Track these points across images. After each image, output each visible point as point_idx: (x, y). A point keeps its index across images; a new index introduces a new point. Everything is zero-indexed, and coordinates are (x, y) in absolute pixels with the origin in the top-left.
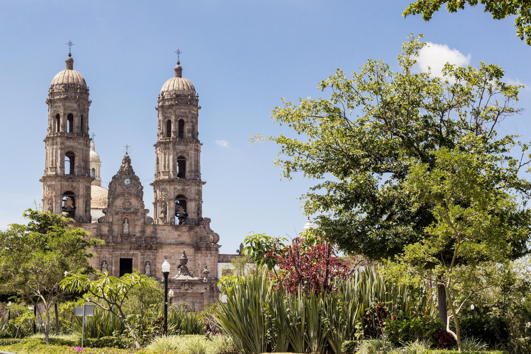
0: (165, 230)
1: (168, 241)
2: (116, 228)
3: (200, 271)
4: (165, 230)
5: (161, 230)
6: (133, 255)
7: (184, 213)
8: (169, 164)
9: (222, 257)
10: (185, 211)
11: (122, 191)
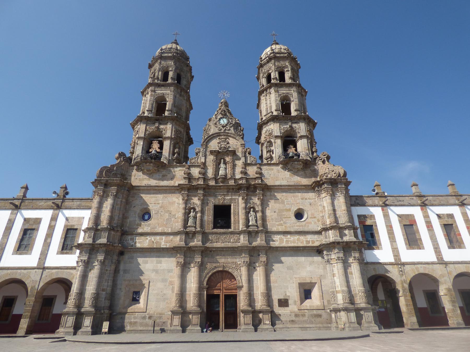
0: (273, 169)
1: (277, 183)
3: (327, 216)
6: (231, 199)
9: (354, 199)
10: (296, 150)
11: (217, 131)
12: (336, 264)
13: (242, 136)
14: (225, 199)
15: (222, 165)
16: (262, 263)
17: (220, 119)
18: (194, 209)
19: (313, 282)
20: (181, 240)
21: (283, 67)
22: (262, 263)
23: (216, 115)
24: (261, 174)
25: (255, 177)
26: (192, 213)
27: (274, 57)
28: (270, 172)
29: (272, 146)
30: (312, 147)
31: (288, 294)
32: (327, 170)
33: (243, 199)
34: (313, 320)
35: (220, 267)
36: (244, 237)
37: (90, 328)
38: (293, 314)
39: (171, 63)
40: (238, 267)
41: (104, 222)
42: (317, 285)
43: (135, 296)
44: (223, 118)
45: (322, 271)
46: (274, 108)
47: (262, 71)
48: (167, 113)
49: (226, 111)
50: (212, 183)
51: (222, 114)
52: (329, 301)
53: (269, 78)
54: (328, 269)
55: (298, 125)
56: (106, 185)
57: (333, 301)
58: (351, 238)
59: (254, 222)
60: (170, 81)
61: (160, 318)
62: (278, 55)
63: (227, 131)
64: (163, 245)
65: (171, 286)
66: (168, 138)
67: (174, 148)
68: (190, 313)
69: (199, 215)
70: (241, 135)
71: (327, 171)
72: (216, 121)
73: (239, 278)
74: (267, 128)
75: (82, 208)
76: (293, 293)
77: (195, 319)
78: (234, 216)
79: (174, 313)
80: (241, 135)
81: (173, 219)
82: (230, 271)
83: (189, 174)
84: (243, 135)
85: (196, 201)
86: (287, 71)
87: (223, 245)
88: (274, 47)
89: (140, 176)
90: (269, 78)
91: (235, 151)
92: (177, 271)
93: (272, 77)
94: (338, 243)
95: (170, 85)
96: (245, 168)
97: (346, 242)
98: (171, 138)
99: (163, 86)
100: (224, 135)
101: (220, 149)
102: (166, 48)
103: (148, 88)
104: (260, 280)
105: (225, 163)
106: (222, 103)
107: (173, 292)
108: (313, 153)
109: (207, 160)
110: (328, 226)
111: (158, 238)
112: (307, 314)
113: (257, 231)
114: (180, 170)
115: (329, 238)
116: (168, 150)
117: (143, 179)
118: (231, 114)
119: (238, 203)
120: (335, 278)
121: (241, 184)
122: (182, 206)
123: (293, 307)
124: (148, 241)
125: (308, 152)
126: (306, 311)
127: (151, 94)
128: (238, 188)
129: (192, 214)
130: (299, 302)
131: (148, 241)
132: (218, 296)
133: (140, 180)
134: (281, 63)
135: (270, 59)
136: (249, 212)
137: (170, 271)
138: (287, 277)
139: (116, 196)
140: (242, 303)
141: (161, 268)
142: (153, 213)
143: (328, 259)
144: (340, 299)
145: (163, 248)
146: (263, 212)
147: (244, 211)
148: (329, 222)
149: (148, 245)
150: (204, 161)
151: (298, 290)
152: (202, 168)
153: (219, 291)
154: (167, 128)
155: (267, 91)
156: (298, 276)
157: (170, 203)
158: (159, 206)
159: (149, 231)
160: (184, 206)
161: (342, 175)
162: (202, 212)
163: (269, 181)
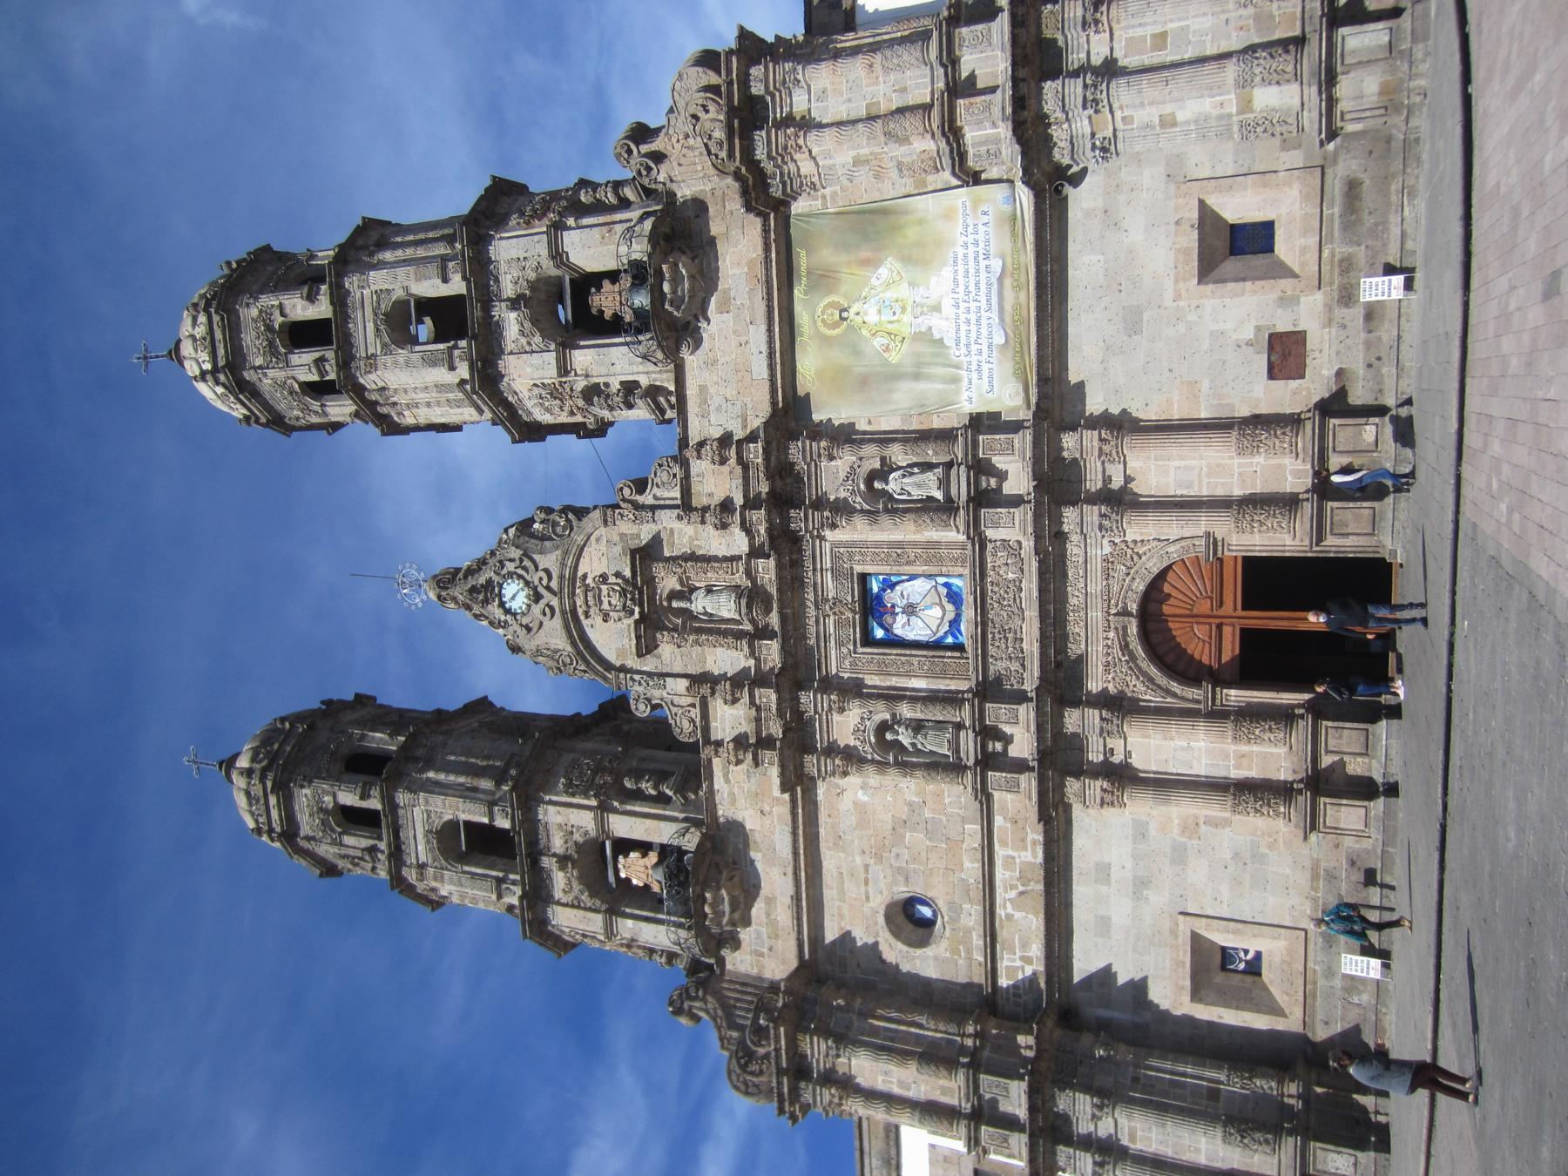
0: (703, 389)
1: (760, 369)
2: (727, 659)
3: (898, 151)
4: (703, 389)
5: (704, 415)
7: (626, 281)
8: (440, 387)
10: (613, 276)
11: (557, 622)
12: (1118, 114)
13: (570, 516)
14: (836, 600)
15: (700, 604)
16: (1106, 448)
17: (508, 611)
18: (883, 728)
19: (1194, 215)
20: (1013, 788)
21: (269, 328)
22: (1106, 448)
23: (491, 623)
24: (725, 440)
25: (739, 470)
26: (900, 738)
27: (232, 371)
28: (715, 402)
29: (607, 385)
30: (599, 208)
31: (1248, 333)
32: (691, 141)
33: (834, 526)
34: (1369, 221)
35: (1125, 628)
36: (996, 525)
37: (1360, 1154)
38: (1340, 313)
39: (304, 796)
40: (1127, 554)
41: (948, 1088)
42: (1212, 201)
43: (1242, 966)
44: (500, 595)
45: (1146, 173)
46: (441, 375)
47: (298, 419)
48: (503, 823)
49: (471, 582)
50: (772, 653)
51: (486, 602)
52: (1286, 145)
53: (320, 390)
54: (1137, 148)
55: (503, 267)
56: (799, 1070)
57: (1285, 128)
58: (995, 38)
59: (931, 478)
60: (374, 804)
61: (1331, 877)
62: (221, 351)
63: (554, 584)
64: (1033, 855)
65: (1203, 828)
66: (601, 824)
67: (638, 796)
68: (1315, 759)
69: (906, 711)
70: (568, 520)
71: (696, 142)
72: (517, 627)
73: (1171, 549)
74: (529, 404)
75: (893, 1152)
76: (1244, 309)
77: (1344, 744)
78: (908, 563)
79: (1313, 823)
80: (568, 520)
81: (928, 814)
82: (1140, 586)
83: (740, 742)
84: (565, 510)
85: (847, 725)
86: (283, 314)
87: (1032, 613)
88: (192, 369)
89: (758, 933)
90: (320, 390)
91: (633, 552)
92: (1139, 806)
93: (314, 377)
94: (1019, 102)
95: (392, 807)
96: (705, 509)
97: (1014, 64)
98: (604, 808)
99: (396, 830)
100: (574, 594)
101: (632, 613)
102: (252, 814)
103: (411, 887)
104: (1181, 458)
105: (687, 593)
106: (439, 597)
107: (1226, 823)
108: (625, 204)
109: (677, 670)
110: (943, 144)
111: (1000, 875)
112: (1342, 250)
113: (969, 468)
114: (727, 781)
115: (997, 141)
116: (648, 822)
117: (772, 923)
118: (482, 562)
119: (853, 544)
120: (1180, 116)
121: (769, 531)
122: (872, 777)
123: (1307, 312)
124: (1018, 915)
125: (619, 228)
126: (1326, 253)
127: (435, 879)
128: (786, 546)
129: (905, 738)
130: (1286, 284)
131: (1018, 915)
132: (1247, 636)
133: (777, 936)
134: (251, 339)
135: (242, 388)
136: (889, 497)
137: (1140, 832)
138: (1170, 347)
139: (843, 1038)
140: (1283, 539)
141: (1129, 865)
142: (902, 891)
143: (1094, 147)
144: (1280, 97)
145: (1049, 858)
146: (884, 439)
147: (885, 520)
148: (924, 145)
149: (1036, 914)
150: (684, 683)
151: (1231, 286)
152: (713, 693)
153: (1227, 630)
154: (560, 826)
155: (376, 403)
156: (1169, 284)
157: (862, 824)
158: (876, 869)
159: (980, 908)
160: (871, 769)
161: (714, 79)
162: (892, 696)
163: (757, 410)
